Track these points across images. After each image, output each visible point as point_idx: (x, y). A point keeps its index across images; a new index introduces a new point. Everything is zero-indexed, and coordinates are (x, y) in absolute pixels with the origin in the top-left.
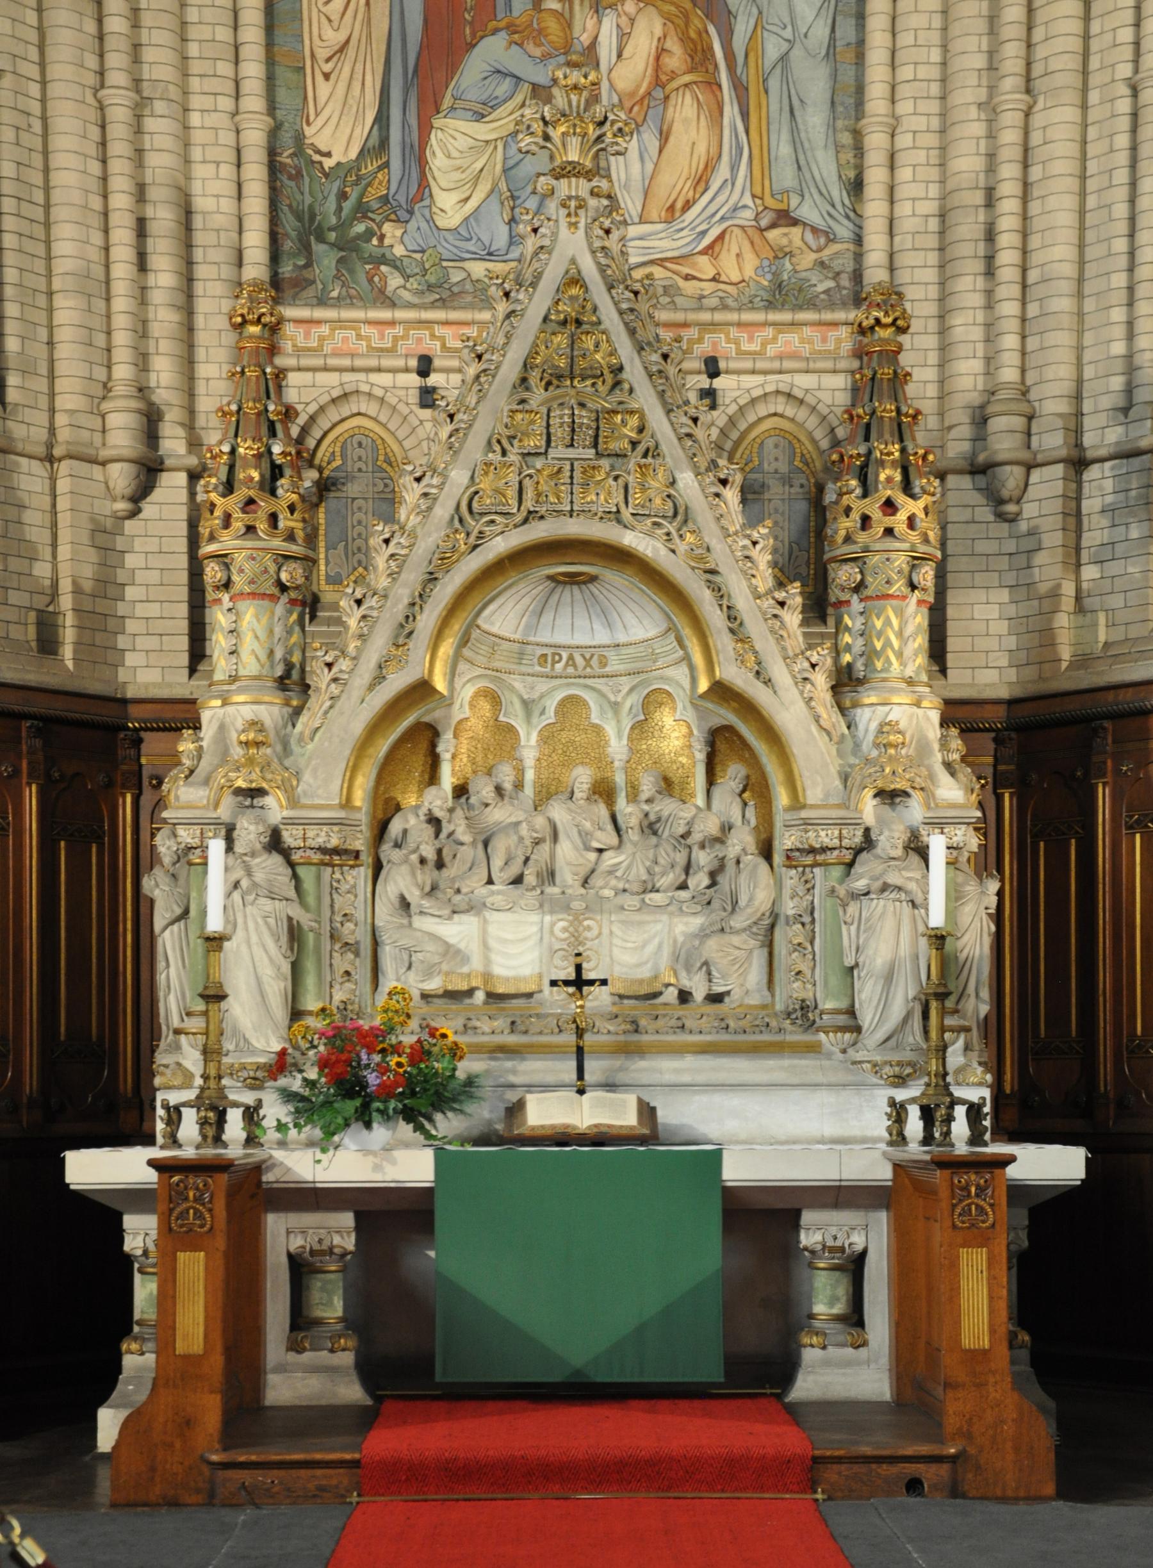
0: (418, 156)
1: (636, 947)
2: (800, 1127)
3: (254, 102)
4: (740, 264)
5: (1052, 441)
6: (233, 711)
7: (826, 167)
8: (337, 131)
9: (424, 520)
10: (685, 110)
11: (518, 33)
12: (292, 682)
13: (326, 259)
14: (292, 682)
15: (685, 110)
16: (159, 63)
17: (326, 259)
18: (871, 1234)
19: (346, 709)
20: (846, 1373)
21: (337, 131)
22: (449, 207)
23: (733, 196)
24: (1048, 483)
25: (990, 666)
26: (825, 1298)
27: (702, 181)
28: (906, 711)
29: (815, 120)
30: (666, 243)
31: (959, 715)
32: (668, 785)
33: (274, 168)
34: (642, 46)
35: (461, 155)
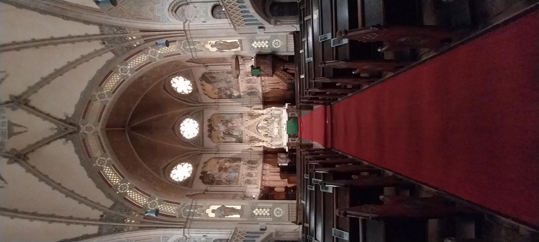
2: (285, 116)
4: (240, 119)
6: (265, 144)
8: (234, 140)
9: (255, 135)
10: (233, 122)
12: (263, 141)
14: (263, 141)
15: (233, 122)
18: (290, 113)
19: (264, 139)
20: (297, 115)
21: (234, 140)
22: (238, 134)
23: (237, 120)
25: (261, 106)
26: (293, 115)
28: (264, 111)
31: (264, 109)
35: (235, 133)
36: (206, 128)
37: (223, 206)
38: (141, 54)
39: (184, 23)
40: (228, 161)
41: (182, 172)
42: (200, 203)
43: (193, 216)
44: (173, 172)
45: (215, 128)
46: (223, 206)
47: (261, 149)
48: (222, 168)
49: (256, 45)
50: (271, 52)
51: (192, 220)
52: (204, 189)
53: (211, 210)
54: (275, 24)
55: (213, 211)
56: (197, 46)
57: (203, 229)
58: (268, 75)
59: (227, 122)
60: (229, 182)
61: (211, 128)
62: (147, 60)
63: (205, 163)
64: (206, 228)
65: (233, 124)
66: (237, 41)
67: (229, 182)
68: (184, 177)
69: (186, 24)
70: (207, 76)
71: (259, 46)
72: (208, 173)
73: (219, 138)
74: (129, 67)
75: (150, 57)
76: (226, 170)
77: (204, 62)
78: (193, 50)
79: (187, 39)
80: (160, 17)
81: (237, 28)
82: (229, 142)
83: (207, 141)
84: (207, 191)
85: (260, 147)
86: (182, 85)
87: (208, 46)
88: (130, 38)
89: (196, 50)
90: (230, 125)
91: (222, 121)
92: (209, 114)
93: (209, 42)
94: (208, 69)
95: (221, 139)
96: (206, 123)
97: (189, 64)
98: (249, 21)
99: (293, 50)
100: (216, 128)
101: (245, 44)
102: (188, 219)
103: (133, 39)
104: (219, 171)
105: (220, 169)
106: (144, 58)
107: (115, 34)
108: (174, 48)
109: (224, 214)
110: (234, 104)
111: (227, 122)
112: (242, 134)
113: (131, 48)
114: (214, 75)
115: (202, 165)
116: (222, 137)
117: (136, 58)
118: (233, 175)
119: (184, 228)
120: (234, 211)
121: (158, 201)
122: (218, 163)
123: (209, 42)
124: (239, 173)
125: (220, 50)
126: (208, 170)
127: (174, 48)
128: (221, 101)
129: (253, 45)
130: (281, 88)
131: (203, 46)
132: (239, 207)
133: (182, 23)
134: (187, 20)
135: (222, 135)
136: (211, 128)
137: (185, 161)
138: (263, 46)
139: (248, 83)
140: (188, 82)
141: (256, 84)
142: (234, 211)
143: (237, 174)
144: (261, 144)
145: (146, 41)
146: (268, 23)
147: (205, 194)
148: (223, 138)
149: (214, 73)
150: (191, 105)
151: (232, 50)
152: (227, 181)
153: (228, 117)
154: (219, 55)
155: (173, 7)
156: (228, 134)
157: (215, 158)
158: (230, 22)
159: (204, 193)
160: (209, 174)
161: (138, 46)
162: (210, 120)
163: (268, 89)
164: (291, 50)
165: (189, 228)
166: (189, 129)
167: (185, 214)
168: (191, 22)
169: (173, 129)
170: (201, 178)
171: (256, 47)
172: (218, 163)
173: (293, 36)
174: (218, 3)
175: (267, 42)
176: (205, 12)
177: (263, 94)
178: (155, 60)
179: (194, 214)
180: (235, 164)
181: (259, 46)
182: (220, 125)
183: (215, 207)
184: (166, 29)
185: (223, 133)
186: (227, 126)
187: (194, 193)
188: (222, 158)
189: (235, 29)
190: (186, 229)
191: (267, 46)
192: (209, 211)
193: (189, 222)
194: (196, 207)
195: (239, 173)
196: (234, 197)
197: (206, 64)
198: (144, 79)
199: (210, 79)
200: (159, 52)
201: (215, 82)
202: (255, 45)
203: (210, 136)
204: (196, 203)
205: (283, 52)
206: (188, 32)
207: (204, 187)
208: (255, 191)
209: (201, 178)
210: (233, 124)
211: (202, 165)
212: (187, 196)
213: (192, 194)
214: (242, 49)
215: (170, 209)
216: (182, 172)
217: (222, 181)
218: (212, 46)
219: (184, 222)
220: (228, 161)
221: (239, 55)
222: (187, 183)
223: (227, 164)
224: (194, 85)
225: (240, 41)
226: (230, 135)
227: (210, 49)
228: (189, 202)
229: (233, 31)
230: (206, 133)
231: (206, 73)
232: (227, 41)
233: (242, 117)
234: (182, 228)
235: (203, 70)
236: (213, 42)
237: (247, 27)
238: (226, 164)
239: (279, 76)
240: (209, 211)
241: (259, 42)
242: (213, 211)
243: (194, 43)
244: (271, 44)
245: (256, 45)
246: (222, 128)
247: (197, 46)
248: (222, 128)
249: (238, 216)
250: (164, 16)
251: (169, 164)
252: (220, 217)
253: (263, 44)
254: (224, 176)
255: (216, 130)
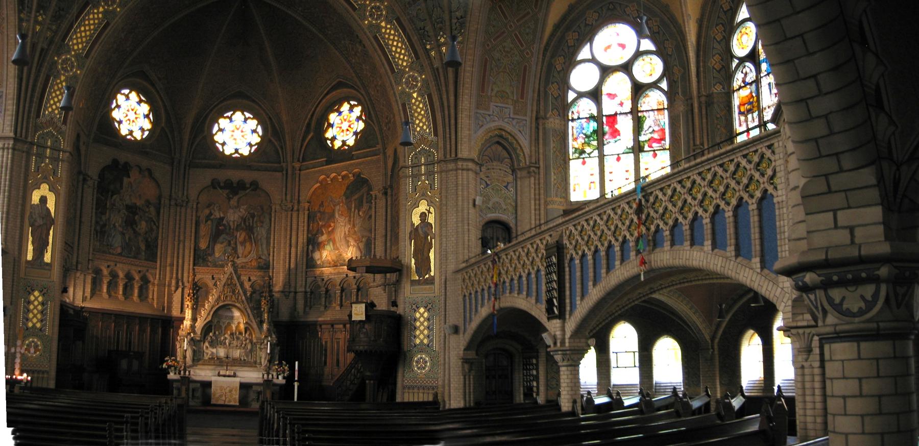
0: (213, 249)
1: (237, 353)
3: (193, 242)
4: (254, 264)
5: (292, 290)
6: (187, 323)
7: (266, 252)
8: (203, 245)
10: (248, 244)
11: (227, 234)
13: (201, 261)
15: (248, 244)
16: (182, 238)
17: (201, 261)
22: (217, 255)
23: (253, 255)
24: (292, 295)
27: (250, 253)
29: (264, 246)
30: (244, 260)
32: (241, 333)
33: (195, 250)
34: (243, 236)
35: (219, 249)
36: (235, 175)
37: (52, 222)
38: (409, 56)
39: (473, 160)
40: (152, 230)
41: (132, 115)
42: (62, 170)
43: (38, 155)
44: (134, 96)
45: (236, 198)
46: (52, 222)
47: (175, 312)
48: (135, 214)
49: (422, 315)
50: (405, 349)
51: (29, 154)
52: (90, 174)
53: (44, 195)
54: (465, 361)
55: (43, 200)
56: (424, 181)
57: (11, 181)
58: (353, 340)
59: (250, 230)
60: (101, 232)
61: (234, 188)
62: (397, 65)
63: (149, 170)
64: (10, 187)
65: (243, 243)
66: (432, 274)
67: (101, 232)
68: (120, 122)
69: (471, 165)
70: (365, 189)
71: (418, 324)
72: (126, 180)
73: (209, 206)
74: (383, 24)
75: (404, 72)
76: (130, 223)
77: (392, 190)
78: (415, 169)
79: (439, 162)
80: (487, 109)
81: (459, 276)
82: (197, 232)
83: (201, 178)
84: (84, 180)
85: (182, 310)
86: (345, 126)
87: (423, 207)
88: (442, 40)
89: (417, 177)
90: (241, 236)
91: (253, 216)
92: (271, 184)
93: (432, 210)
94: (380, 195)
95: (207, 211)
96: (247, 176)
97: (390, 152)
98: (470, 302)
99: (406, 400)
100: (233, 202)
101: (422, 293)
102: (32, 144)
103: (440, 46)
104: (128, 207)
105: (132, 210)
106: (403, 60)
107: (451, 12)
108: (422, 128)
109: (37, 224)
110: (293, 250)
111: (250, 230)
112: (216, 266)
113: (423, 36)
114: (365, 206)
115: (145, 163)
116: (211, 214)
117: (403, 43)
118: (117, 242)
119: (15, 139)
120: (40, 250)
121: (75, 76)
122: (148, 203)
123: (432, 210)
124: (120, 254)
125: (415, 231)
126: (132, 179)
127: (422, 128)
128: (303, 218)
129: (422, 310)
130: (327, 370)
131: (424, 196)
132: (47, 258)
133: (474, 155)
134: (481, 165)
135: (217, 214)
136: (234, 188)
137: (154, 124)
138: (418, 332)
139: (342, 290)
140: (351, 142)
141: (338, 308)
142: (40, 250)
143: (119, 250)
144: (188, 314)
145: (435, 72)
146: (465, 344)
147: (78, 177)
148: (208, 218)
149: (370, 208)
150: (293, 142)
151: (413, 261)
152: (105, 225)
153: (261, 232)
154: (405, 232)
155: (506, 139)
156: (219, 231)
157: (160, 198)
158: (473, 260)
159: (80, 173)
160: (122, 184)
161: (427, 52)
162: (255, 186)
163: (325, 336)
164: (406, 395)
165: (14, 149)
166: (237, 134)
167: (42, 137)
168: (476, 173)
169: (240, 95)
170: (115, 162)
171: (418, 315)
172: (148, 203)
173: (431, 399)
174: (514, 235)
175: (425, 341)
176: (495, 208)
177: (315, 324)
178: (399, 83)
179: (41, 157)
180: (143, 247)
181: (418, 324)
182: (243, 211)
183: (51, 205)
184: (459, 121)
185: (222, 219)
186: (238, 228)
187: (83, 148)
188: (158, 213)
189: (457, 272)
190: (11, 142)
191: (418, 341)
192: (44, 190)
193: (25, 147)
194: (55, 160)
195: (120, 254)
196: (69, 247)
197: (389, 191)
198: (360, 48)
199: (356, 197)
200: (415, 95)
201: (349, 209)
202: (422, 314)
203: (215, 184)
204: (63, 161)
205: (403, 379)
206: (451, 166)
207: (93, 172)
208: (79, 295)
209: (115, 162)
210: (243, 243)
211: (145, 163)
212: (78, 136)
213: (81, 143)
214: (414, 282)
215: (57, 100)
216: (132, 115)
217: (103, 213)
218: (423, 216)
219: (26, 137)
220: (152, 230)
221: (401, 275)
222: (106, 128)
223: (143, 226)
224: (345, 154)
225: (431, 281)
226: (215, 238)
227: (419, 211)
228: (65, 144)
229: (452, 267)
230: (223, 175)
231: (370, 189)
232: (432, 251)
233: (260, 268)
234: (16, 133)
235: (377, 181)
236: (431, 219)
237: (461, 298)
238: (144, 224)
239: (352, 366)
240: (44, 190)
241: (426, 324)
242: (43, 200)
243: (430, 174)
244: (421, 351)
245: (422, 315)
246: (233, 217)
247: (424, 181)
248: (233, 217)
249: (30, 257)
250: (488, 118)
251: (153, 85)
252: (31, 216)
253: (422, 332)
254: (117, 219)
255: (229, 199)
